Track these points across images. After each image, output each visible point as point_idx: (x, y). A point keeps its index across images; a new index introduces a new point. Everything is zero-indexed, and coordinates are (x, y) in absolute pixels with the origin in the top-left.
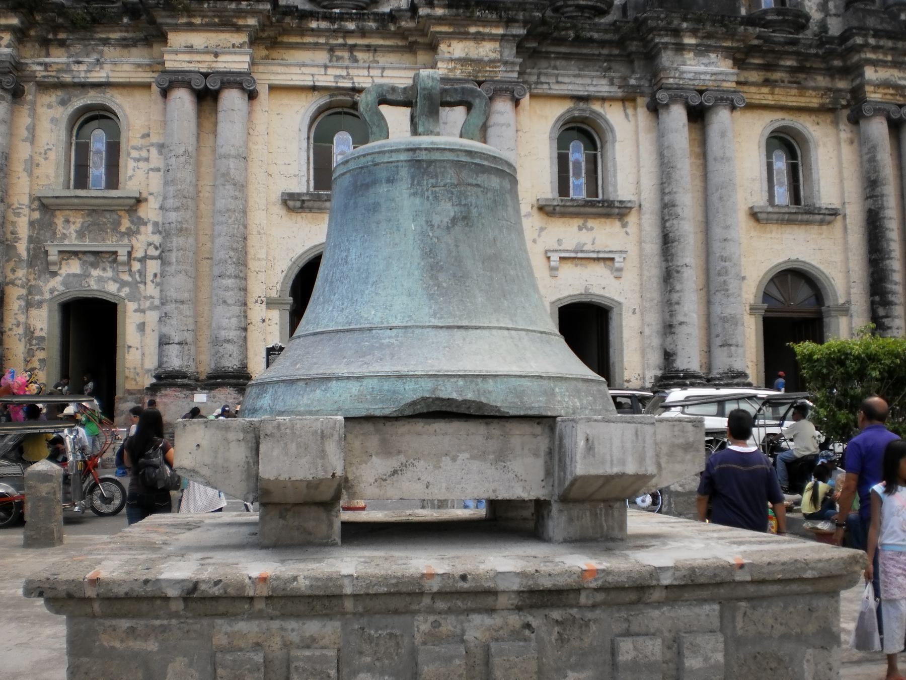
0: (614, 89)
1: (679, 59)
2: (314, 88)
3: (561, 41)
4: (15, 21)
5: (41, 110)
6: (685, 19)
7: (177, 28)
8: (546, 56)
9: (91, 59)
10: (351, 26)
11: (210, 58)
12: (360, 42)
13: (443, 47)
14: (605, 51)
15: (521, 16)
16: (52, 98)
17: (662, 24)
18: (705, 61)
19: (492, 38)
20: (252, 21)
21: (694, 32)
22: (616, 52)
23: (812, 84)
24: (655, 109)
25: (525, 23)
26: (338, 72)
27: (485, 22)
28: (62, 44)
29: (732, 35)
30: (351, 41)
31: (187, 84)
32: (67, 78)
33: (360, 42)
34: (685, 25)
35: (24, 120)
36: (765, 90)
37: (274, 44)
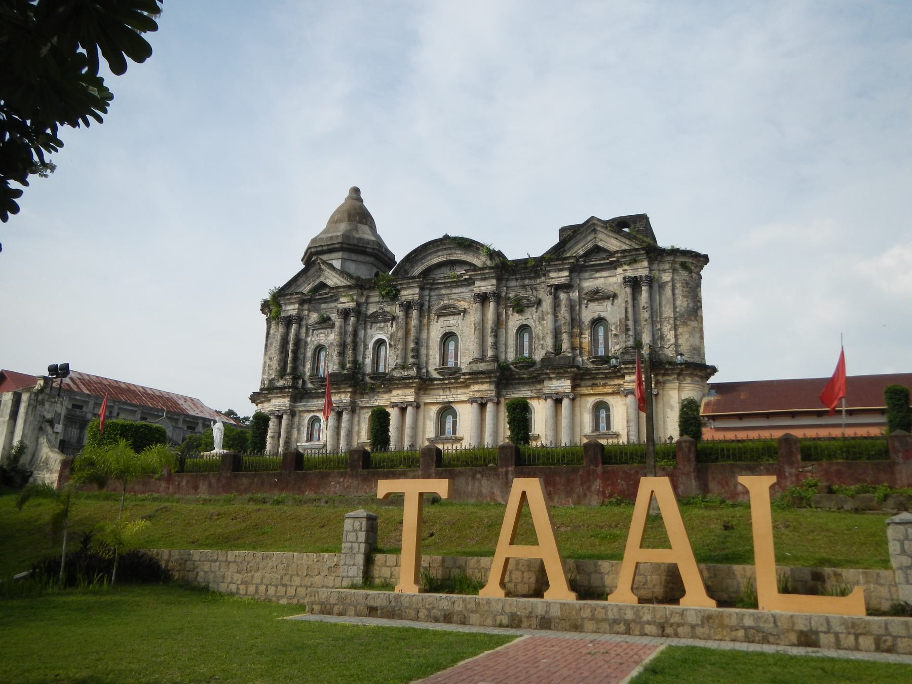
0: (533, 394)
1: (550, 382)
2: (438, 403)
3: (515, 379)
4: (350, 390)
5: (362, 415)
6: (547, 369)
7: (395, 389)
8: (511, 384)
9: (376, 398)
10: (447, 382)
11: (404, 397)
12: (451, 386)
13: (472, 387)
14: (531, 381)
15: (492, 375)
16: (366, 410)
17: (540, 372)
18: (560, 382)
19: (487, 382)
20: (414, 385)
21: (553, 373)
22: (534, 380)
23: (612, 383)
24: (546, 400)
25: (495, 377)
26: (444, 397)
27: (483, 378)
28: (367, 394)
29: (568, 372)
30: (448, 386)
31: (397, 406)
32: (367, 405)
33: (451, 386)
34: (548, 371)
35: (356, 419)
36: (589, 388)
37: (426, 389)
